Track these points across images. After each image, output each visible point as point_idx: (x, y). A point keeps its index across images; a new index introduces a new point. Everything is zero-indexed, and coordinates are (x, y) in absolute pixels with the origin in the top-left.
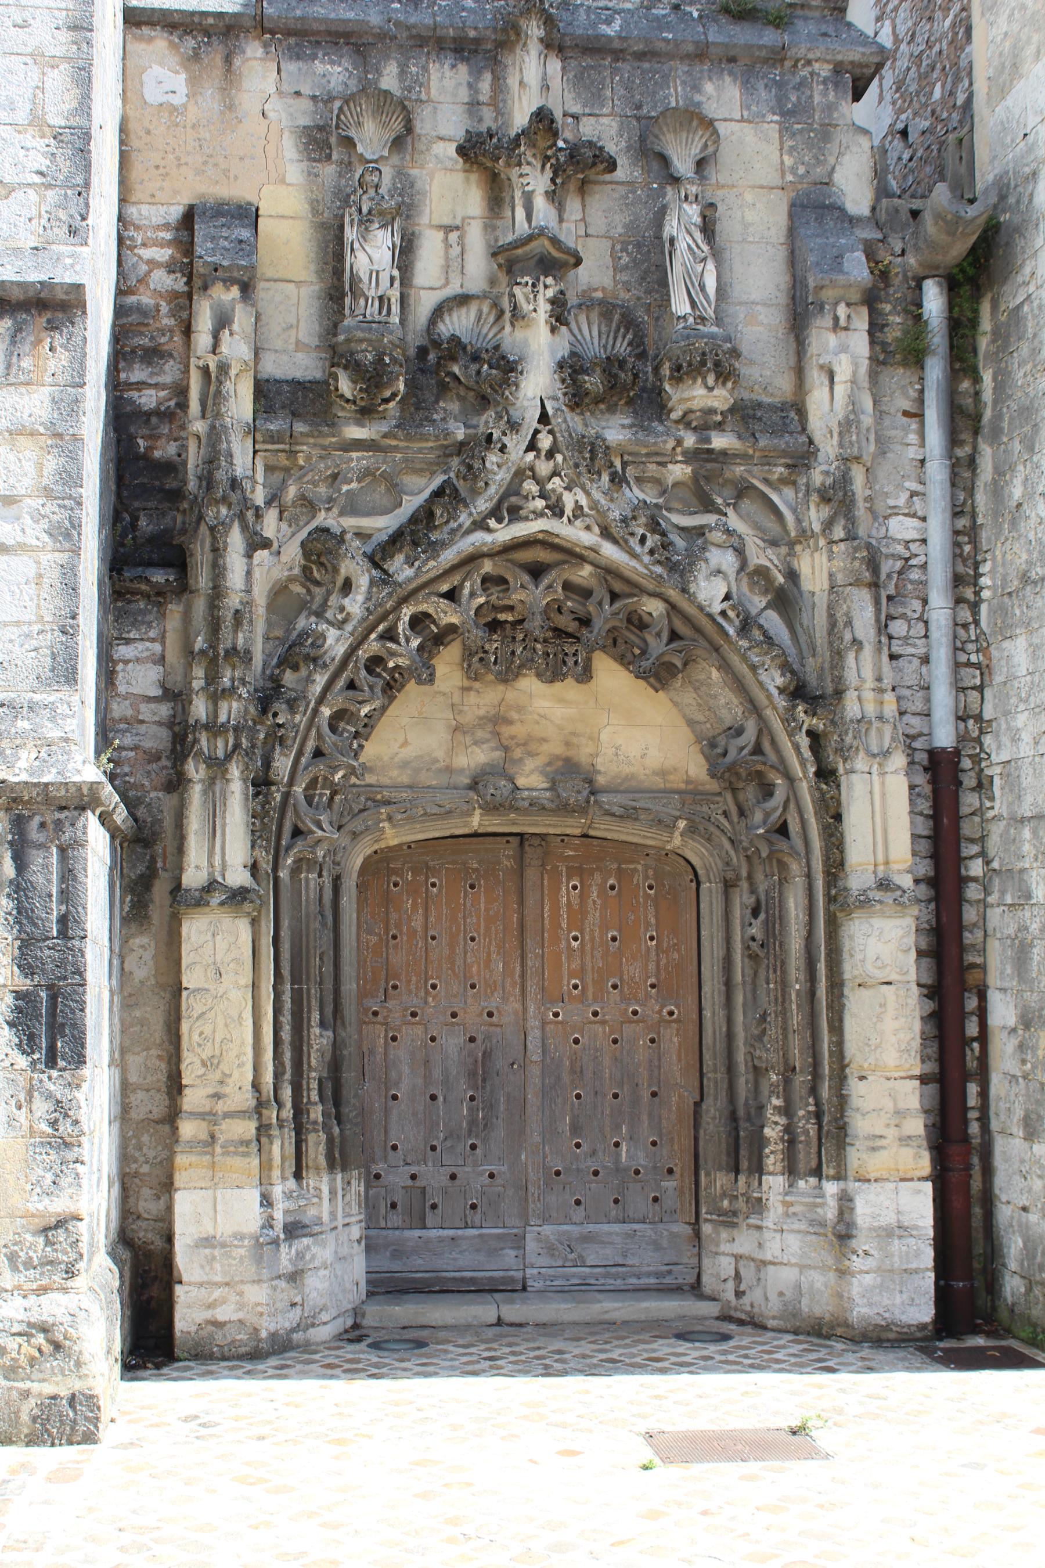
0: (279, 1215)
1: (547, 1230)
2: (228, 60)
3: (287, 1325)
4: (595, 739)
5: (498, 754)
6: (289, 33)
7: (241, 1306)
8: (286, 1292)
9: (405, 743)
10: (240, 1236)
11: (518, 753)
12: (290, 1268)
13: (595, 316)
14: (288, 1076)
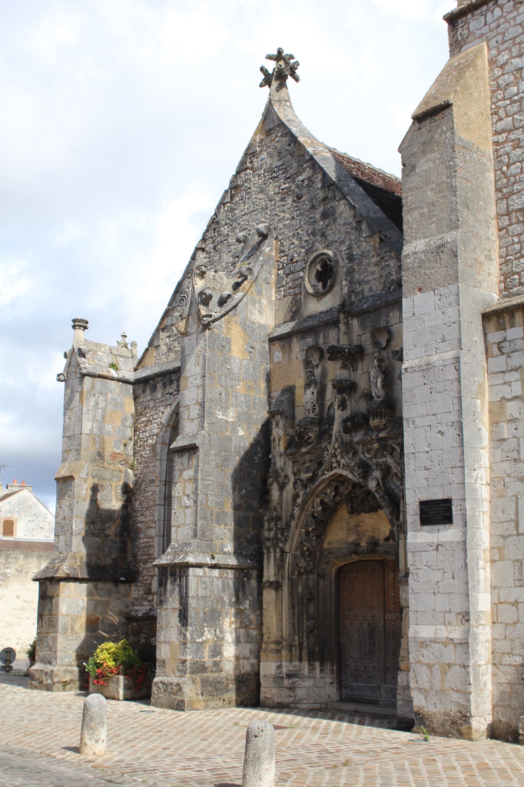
0: (284, 670)
1: (386, 685)
2: (290, 345)
3: (287, 701)
4: (379, 530)
5: (357, 537)
6: (301, 332)
7: (271, 694)
8: (286, 692)
9: (337, 535)
10: (271, 675)
11: (361, 536)
12: (289, 686)
13: (363, 399)
14: (296, 633)
